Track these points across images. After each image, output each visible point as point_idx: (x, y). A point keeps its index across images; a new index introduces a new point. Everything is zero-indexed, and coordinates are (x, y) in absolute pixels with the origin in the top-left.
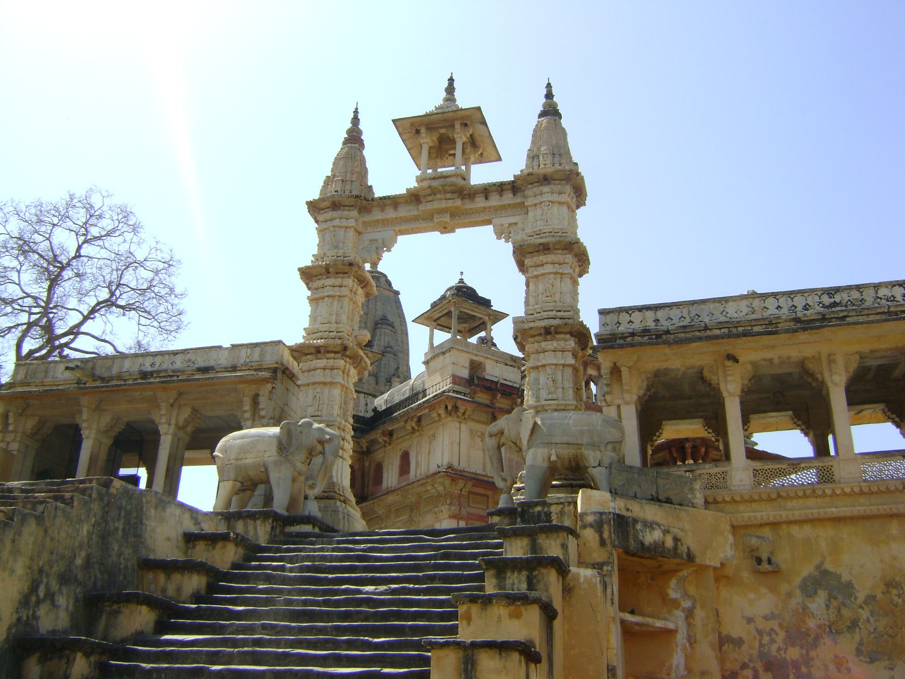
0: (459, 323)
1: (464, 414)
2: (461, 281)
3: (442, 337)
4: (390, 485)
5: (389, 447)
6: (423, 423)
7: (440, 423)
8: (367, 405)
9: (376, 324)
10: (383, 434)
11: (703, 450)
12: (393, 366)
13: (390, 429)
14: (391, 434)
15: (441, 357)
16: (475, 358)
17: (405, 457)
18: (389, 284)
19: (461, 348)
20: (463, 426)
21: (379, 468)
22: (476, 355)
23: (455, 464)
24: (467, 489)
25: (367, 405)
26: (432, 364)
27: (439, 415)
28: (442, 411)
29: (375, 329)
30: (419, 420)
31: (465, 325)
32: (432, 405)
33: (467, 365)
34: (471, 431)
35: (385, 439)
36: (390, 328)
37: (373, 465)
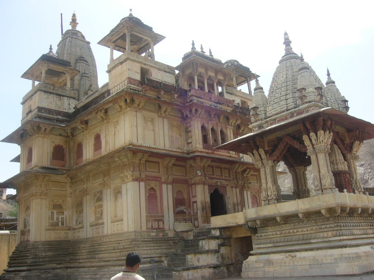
0: (131, 45)
1: (139, 105)
2: (131, 14)
3: (117, 54)
4: (88, 158)
5: (86, 132)
6: (110, 113)
7: (122, 112)
8: (69, 104)
9: (77, 60)
10: (81, 123)
11: (330, 122)
12: (88, 85)
13: (86, 119)
14: (86, 122)
15: (120, 66)
16: (144, 67)
17: (98, 138)
18: (84, 37)
19: (134, 58)
20: (139, 114)
21: (80, 147)
22: (145, 65)
23: (135, 142)
24: (144, 160)
25: (69, 104)
26: (113, 72)
27: (121, 107)
28: (123, 104)
29: (76, 63)
30: (106, 111)
31: (135, 47)
32: (115, 100)
33: (139, 71)
34: (144, 118)
35: (83, 126)
36: (86, 63)
37: (76, 145)
